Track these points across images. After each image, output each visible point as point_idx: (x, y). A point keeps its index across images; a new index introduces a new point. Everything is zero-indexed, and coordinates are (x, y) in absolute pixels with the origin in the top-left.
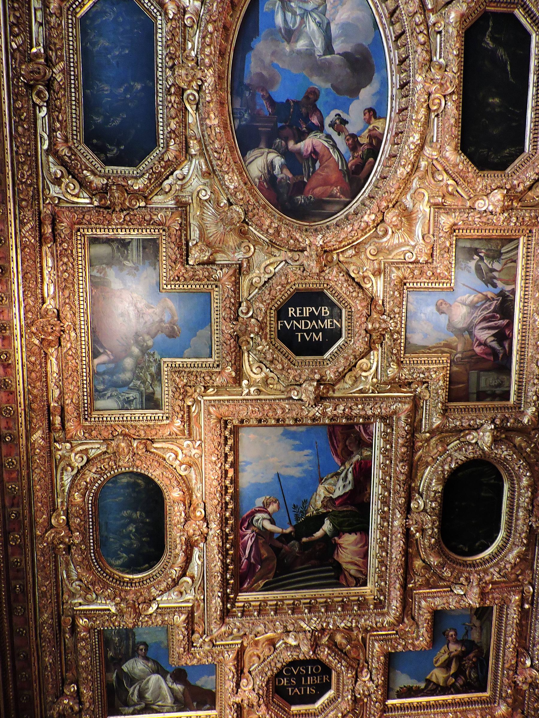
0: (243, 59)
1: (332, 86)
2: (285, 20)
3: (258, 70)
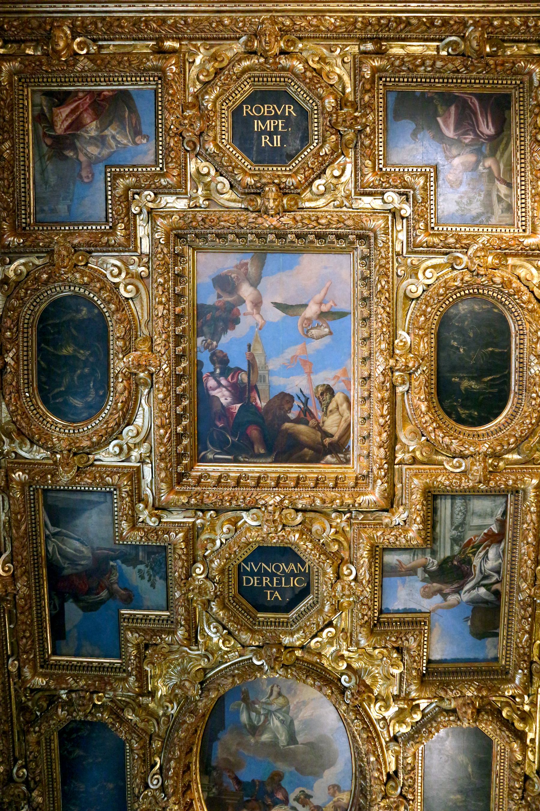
0: (211, 747)
1: (297, 769)
2: (250, 718)
3: (225, 756)
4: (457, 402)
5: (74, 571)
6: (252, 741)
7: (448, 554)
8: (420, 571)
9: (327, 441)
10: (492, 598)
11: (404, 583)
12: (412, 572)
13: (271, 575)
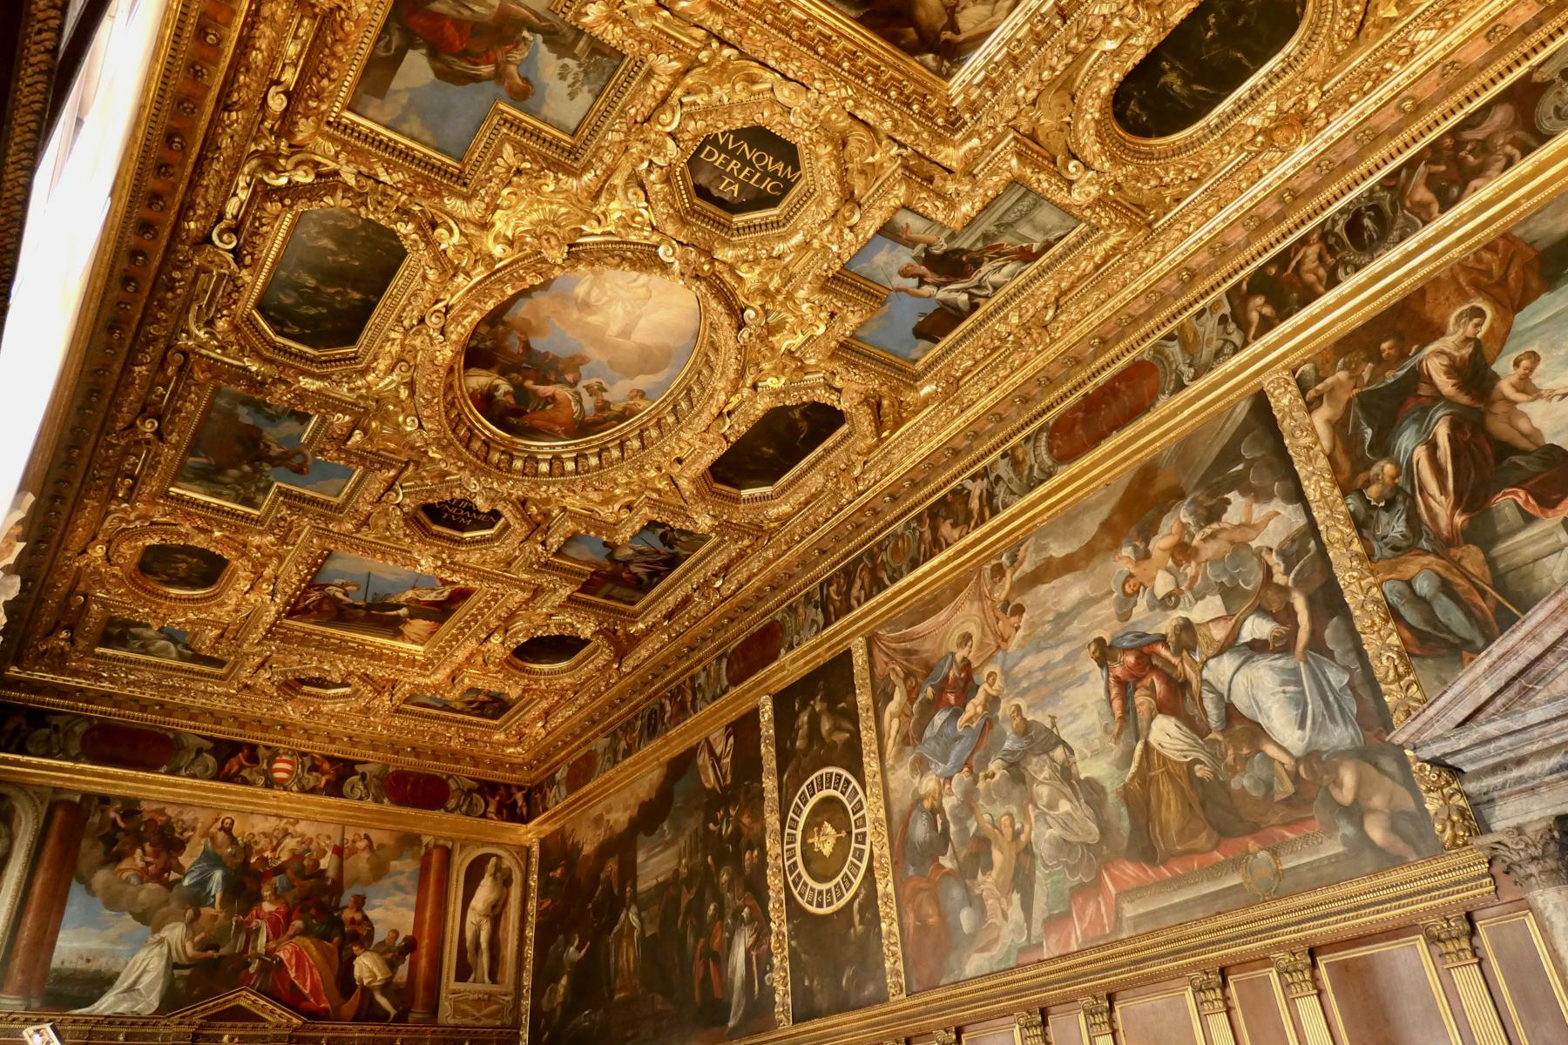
4: (1140, 92)
5: (454, 13)
6: (575, 316)
7: (965, 246)
8: (920, 247)
9: (948, 35)
10: (965, 308)
11: (892, 249)
12: (911, 243)
13: (746, 163)
